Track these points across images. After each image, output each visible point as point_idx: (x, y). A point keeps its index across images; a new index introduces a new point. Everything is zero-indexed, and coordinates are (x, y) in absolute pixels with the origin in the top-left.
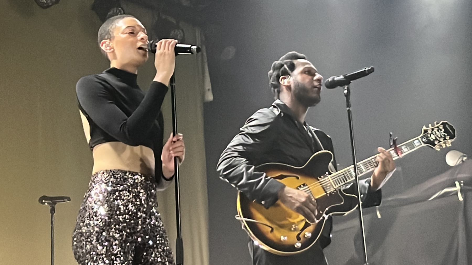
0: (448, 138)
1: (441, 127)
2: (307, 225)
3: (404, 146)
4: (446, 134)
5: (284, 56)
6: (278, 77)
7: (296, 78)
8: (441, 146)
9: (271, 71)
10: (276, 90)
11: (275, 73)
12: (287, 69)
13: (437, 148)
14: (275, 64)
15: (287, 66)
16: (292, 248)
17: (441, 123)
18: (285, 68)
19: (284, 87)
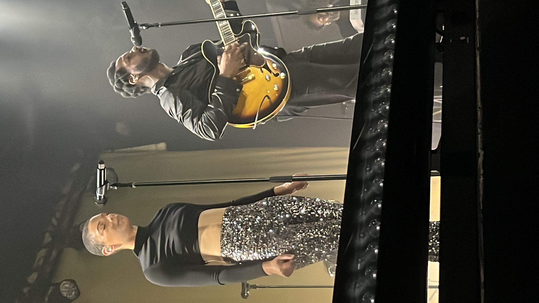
2: (266, 67)
9: (122, 94)
10: (142, 90)
11: (125, 89)
14: (116, 88)
16: (285, 81)
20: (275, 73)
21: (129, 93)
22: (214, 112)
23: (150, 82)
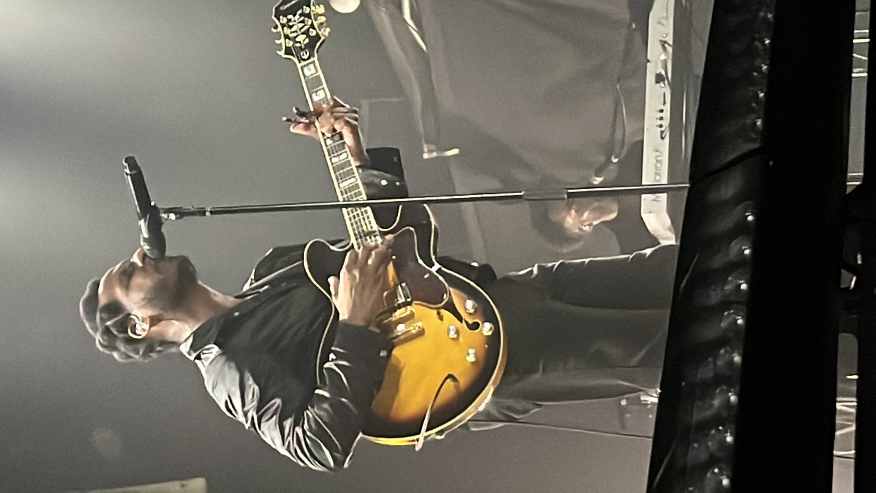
0: (307, 10)
1: (284, 20)
2: (451, 307)
3: (314, 95)
4: (300, 12)
5: (87, 325)
6: (130, 341)
7: (136, 304)
8: (321, 24)
9: (116, 355)
10: (159, 349)
13: (325, 32)
15: (109, 319)
17: (273, 17)
18: (113, 325)
19: (154, 329)
20: (470, 322)
21: (132, 355)
22: (331, 405)
23: (181, 330)
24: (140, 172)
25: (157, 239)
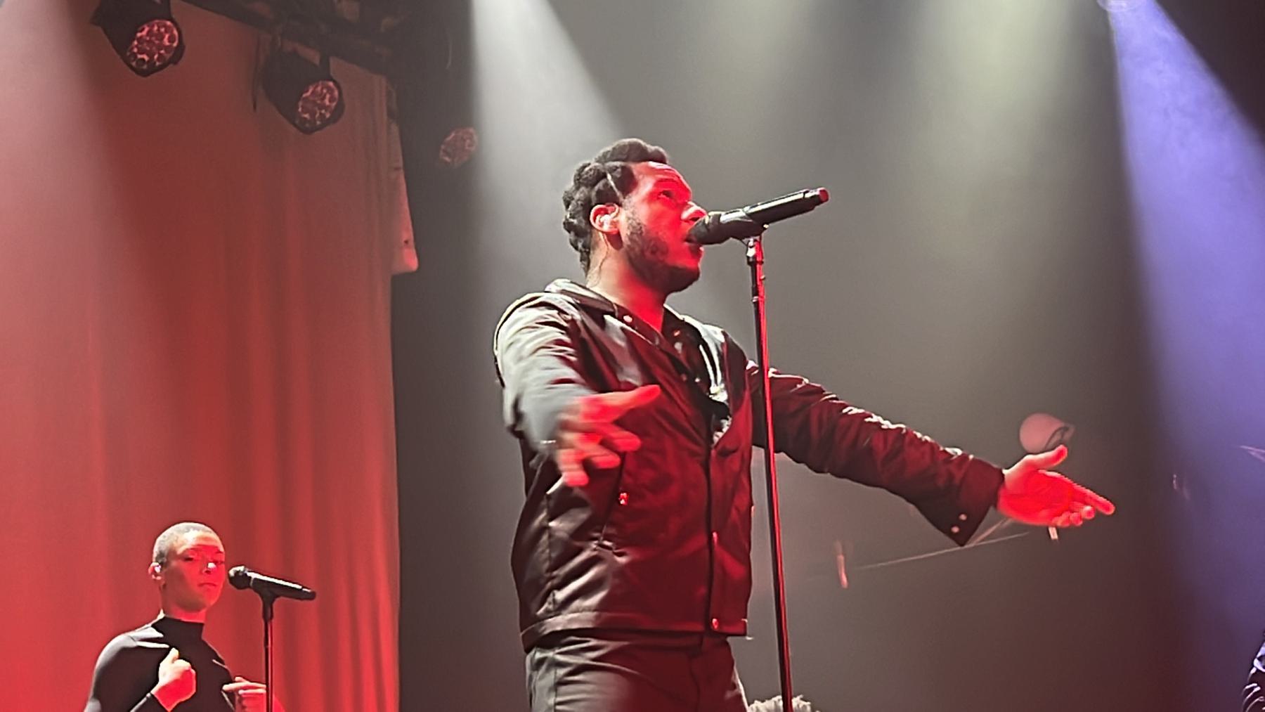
12: (612, 184)
18: (607, 184)
24: (821, 202)
25: (719, 233)
